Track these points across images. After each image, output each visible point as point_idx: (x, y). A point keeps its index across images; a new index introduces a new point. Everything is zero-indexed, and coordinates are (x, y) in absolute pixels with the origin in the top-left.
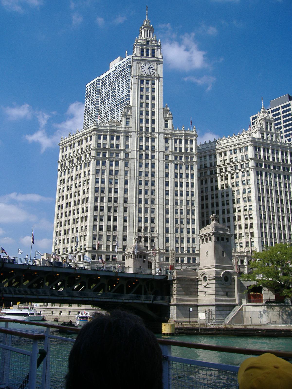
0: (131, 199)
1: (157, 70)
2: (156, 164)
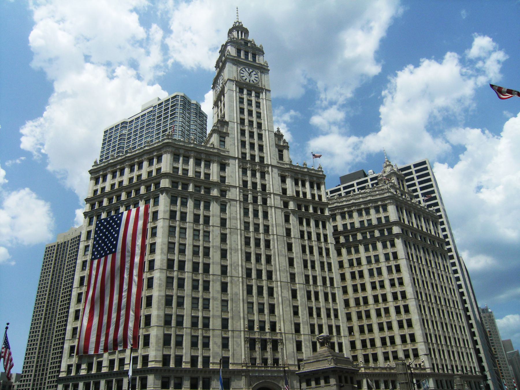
0: (233, 268)
1: (261, 79)
2: (271, 212)
